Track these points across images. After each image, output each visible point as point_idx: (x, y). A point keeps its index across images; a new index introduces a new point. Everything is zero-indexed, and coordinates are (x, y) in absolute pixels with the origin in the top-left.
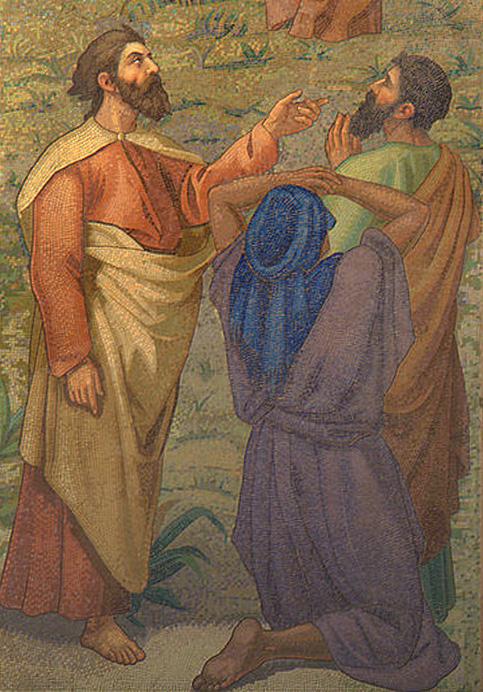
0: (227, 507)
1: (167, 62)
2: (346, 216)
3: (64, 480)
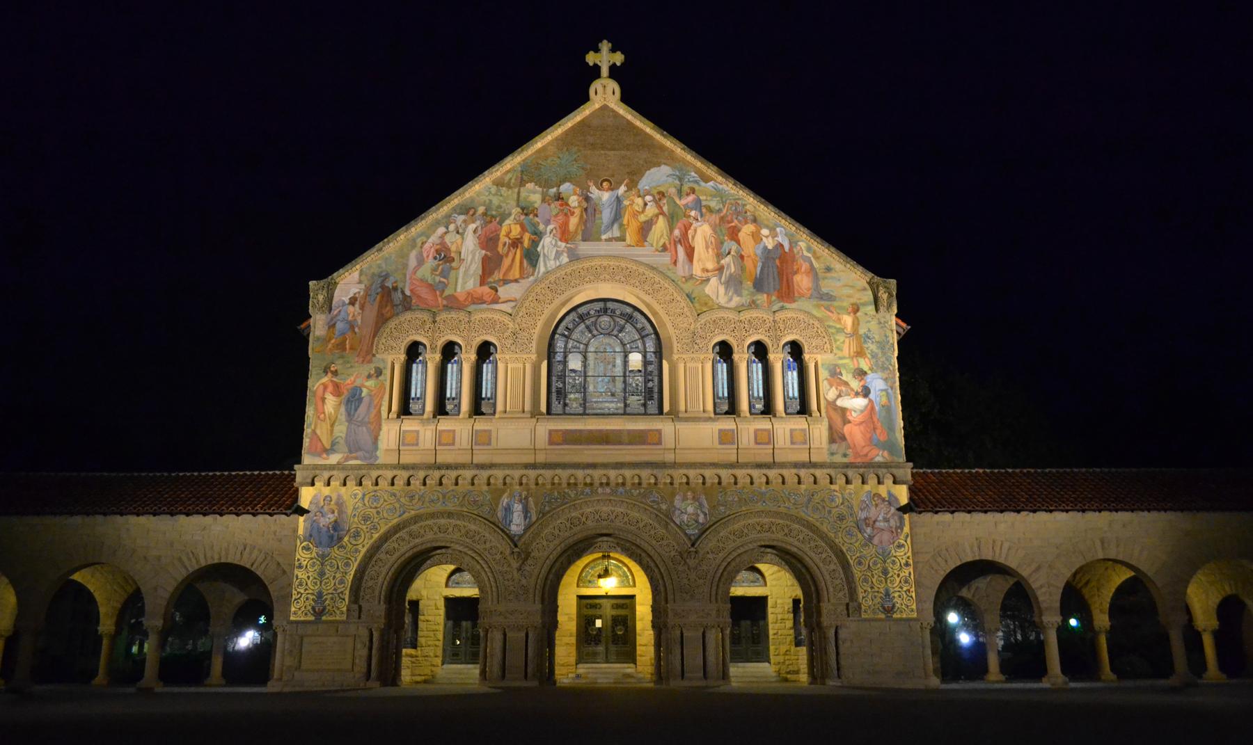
0: (343, 435)
2: (365, 391)
3: (318, 432)
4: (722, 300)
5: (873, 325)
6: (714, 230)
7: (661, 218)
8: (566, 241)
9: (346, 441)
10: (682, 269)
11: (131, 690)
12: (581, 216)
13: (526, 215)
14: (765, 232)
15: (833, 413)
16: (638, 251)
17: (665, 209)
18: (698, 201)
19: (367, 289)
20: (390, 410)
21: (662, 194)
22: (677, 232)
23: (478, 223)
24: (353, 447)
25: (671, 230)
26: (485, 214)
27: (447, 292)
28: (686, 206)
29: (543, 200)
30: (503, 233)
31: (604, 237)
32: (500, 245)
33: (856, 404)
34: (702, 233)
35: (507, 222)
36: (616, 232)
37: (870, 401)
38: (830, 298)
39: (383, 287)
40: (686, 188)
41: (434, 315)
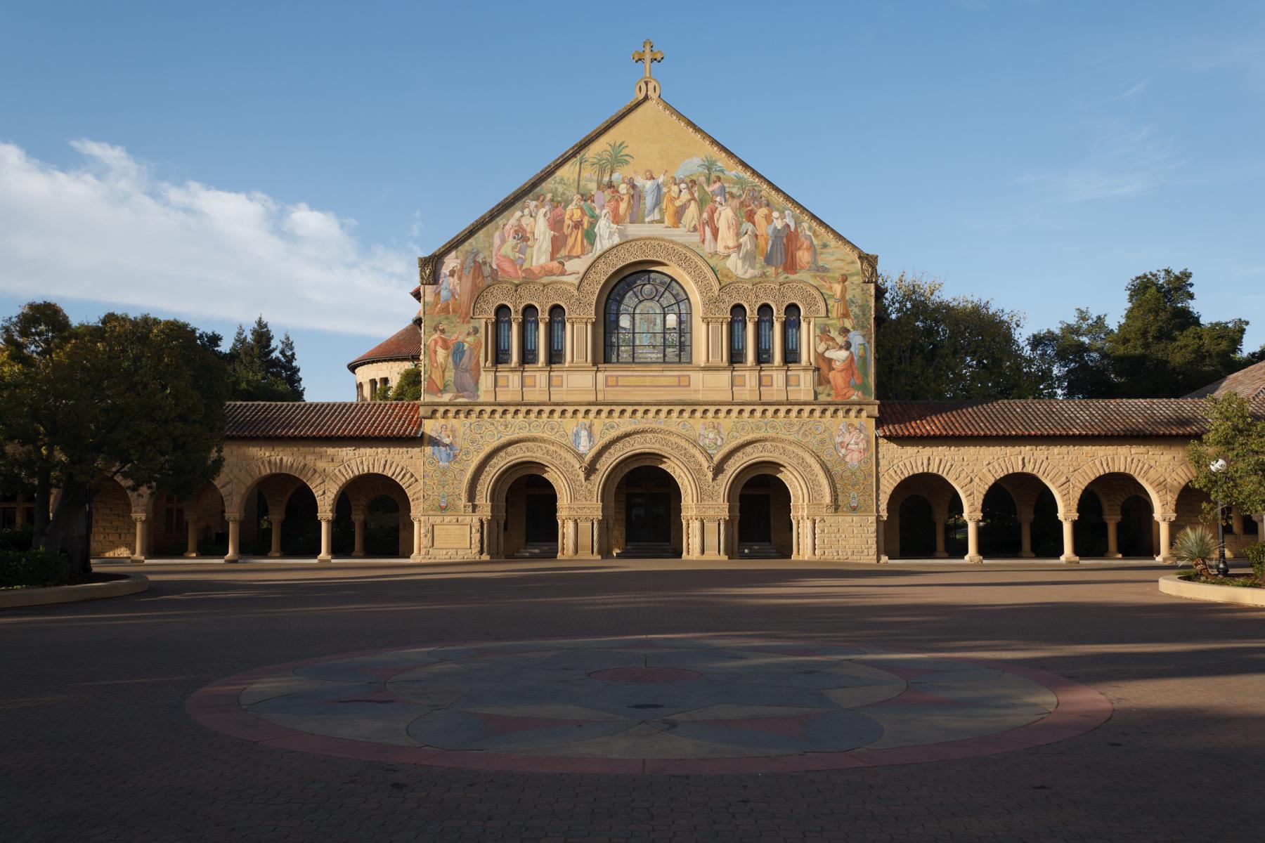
2: (466, 346)
4: (740, 273)
5: (858, 291)
8: (617, 223)
9: (455, 384)
10: (708, 247)
11: (315, 561)
14: (776, 214)
15: (821, 362)
16: (675, 231)
17: (696, 195)
18: (723, 188)
19: (462, 265)
21: (693, 182)
22: (705, 215)
23: (547, 208)
24: (461, 389)
25: (701, 214)
26: (552, 200)
29: (599, 188)
30: (567, 216)
31: (647, 220)
33: (839, 355)
34: (725, 215)
35: (570, 207)
36: (657, 216)
38: (825, 270)
39: (475, 262)
40: (713, 177)
41: (517, 286)
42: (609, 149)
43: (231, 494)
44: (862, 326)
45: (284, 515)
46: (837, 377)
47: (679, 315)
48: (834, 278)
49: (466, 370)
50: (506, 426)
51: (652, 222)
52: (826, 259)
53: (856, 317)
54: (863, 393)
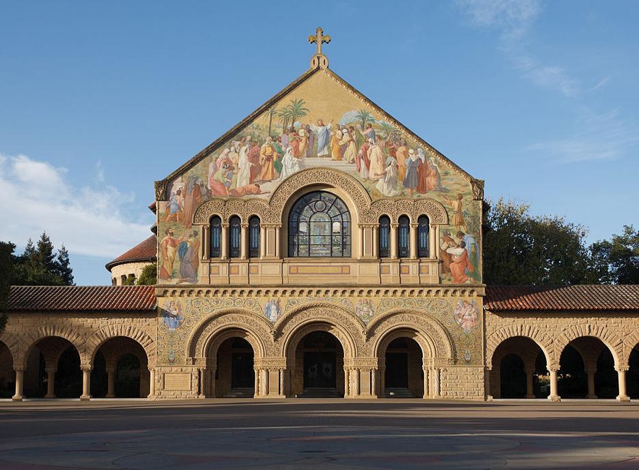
1: (173, 231)
3: (165, 266)
4: (386, 193)
6: (382, 151)
7: (352, 142)
8: (298, 157)
10: (363, 174)
12: (306, 142)
13: (275, 141)
14: (411, 151)
17: (354, 137)
19: (186, 186)
20: (203, 255)
21: (352, 128)
24: (184, 275)
26: (251, 141)
27: (231, 188)
28: (366, 135)
29: (284, 132)
30: (262, 152)
32: (260, 159)
34: (375, 152)
35: (264, 146)
36: (326, 152)
37: (465, 250)
38: (446, 191)
39: (195, 184)
40: (366, 124)
42: (292, 104)
43: (17, 351)
44: (472, 231)
45: (55, 368)
46: (455, 267)
47: (342, 223)
48: (453, 197)
49: (189, 262)
50: (217, 302)
51: (323, 156)
52: (446, 183)
53: (469, 224)
54: (475, 279)
